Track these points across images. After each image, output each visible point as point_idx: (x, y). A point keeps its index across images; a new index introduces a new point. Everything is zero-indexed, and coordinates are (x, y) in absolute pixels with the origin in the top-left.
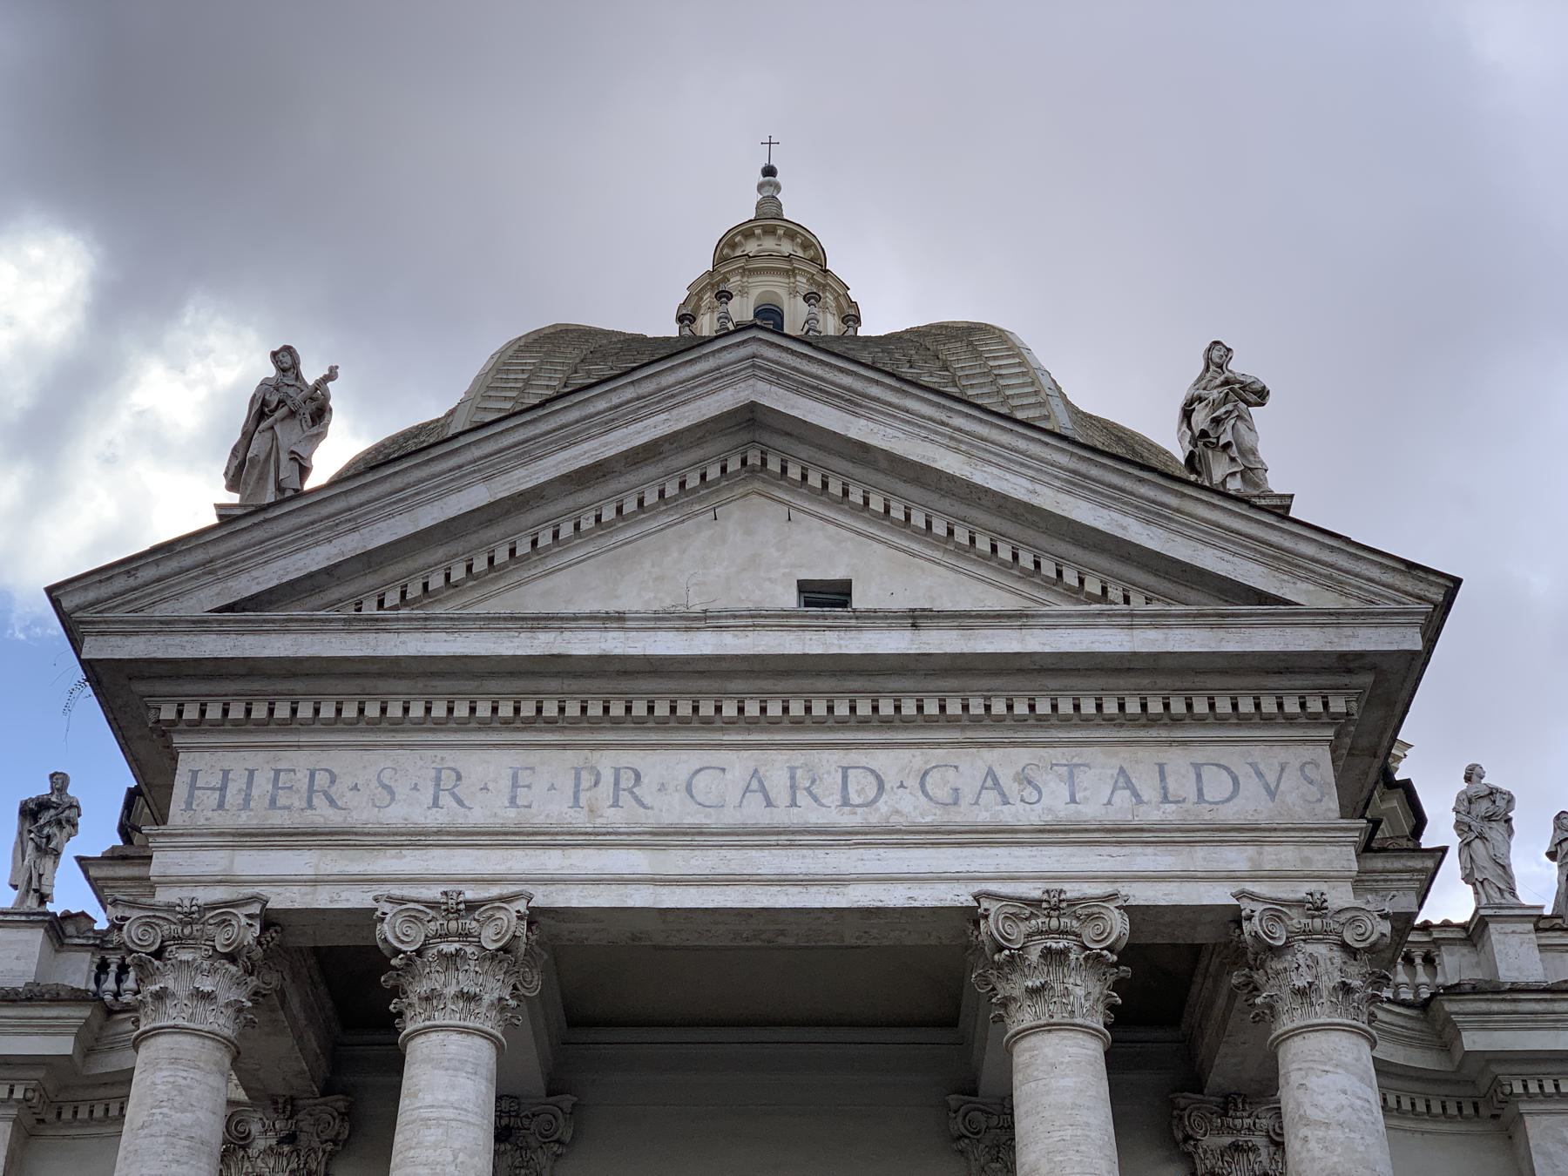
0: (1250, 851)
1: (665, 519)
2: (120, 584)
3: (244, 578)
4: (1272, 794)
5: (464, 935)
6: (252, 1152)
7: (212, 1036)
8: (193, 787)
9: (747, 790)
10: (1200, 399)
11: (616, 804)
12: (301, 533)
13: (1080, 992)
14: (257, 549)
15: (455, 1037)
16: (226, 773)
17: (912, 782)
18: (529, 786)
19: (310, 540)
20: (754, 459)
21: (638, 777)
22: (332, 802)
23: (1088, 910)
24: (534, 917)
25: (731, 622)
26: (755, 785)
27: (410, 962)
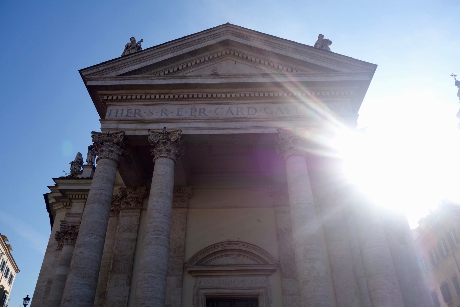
1: (210, 64)
2: (95, 70)
3: (121, 70)
6: (127, 198)
7: (113, 159)
8: (110, 112)
9: (228, 112)
10: (318, 44)
11: (200, 115)
12: (133, 62)
14: (124, 65)
15: (165, 159)
16: (117, 110)
18: (181, 112)
19: (135, 63)
20: (228, 52)
21: (204, 110)
22: (139, 115)
24: (183, 136)
25: (224, 77)
26: (229, 111)
27: (155, 145)
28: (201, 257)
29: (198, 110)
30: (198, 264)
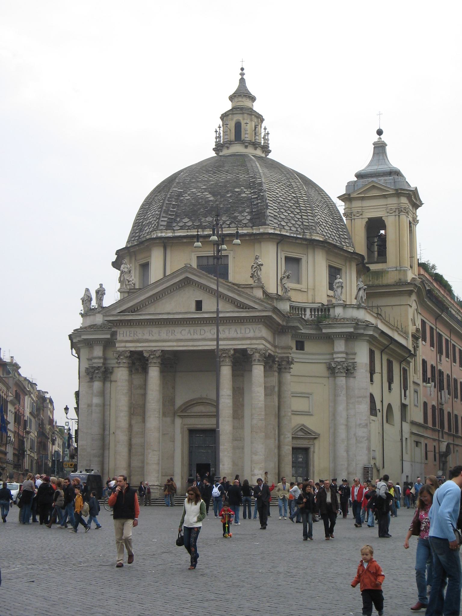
0: (250, 341)
4: (254, 332)
5: (154, 355)
9: (188, 333)
13: (228, 360)
17: (209, 331)
20: (189, 282)
23: (229, 350)
28: (183, 407)
29: (171, 332)
30: (182, 412)
